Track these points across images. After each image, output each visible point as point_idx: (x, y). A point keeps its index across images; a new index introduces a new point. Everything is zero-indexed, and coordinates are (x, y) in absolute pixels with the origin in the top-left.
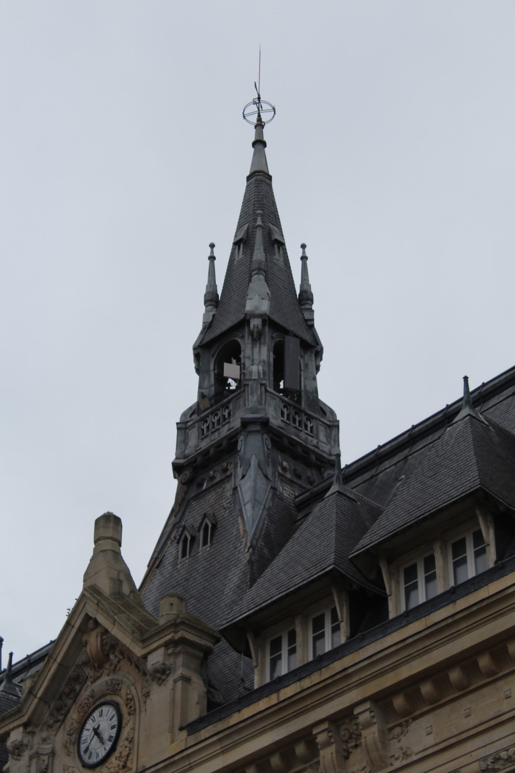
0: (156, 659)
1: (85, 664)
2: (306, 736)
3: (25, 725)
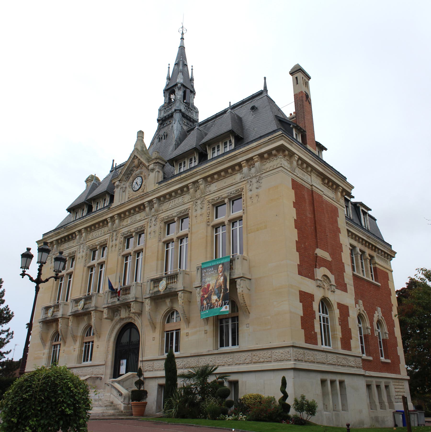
0: (151, 166)
1: (134, 167)
2: (187, 186)
3: (119, 181)
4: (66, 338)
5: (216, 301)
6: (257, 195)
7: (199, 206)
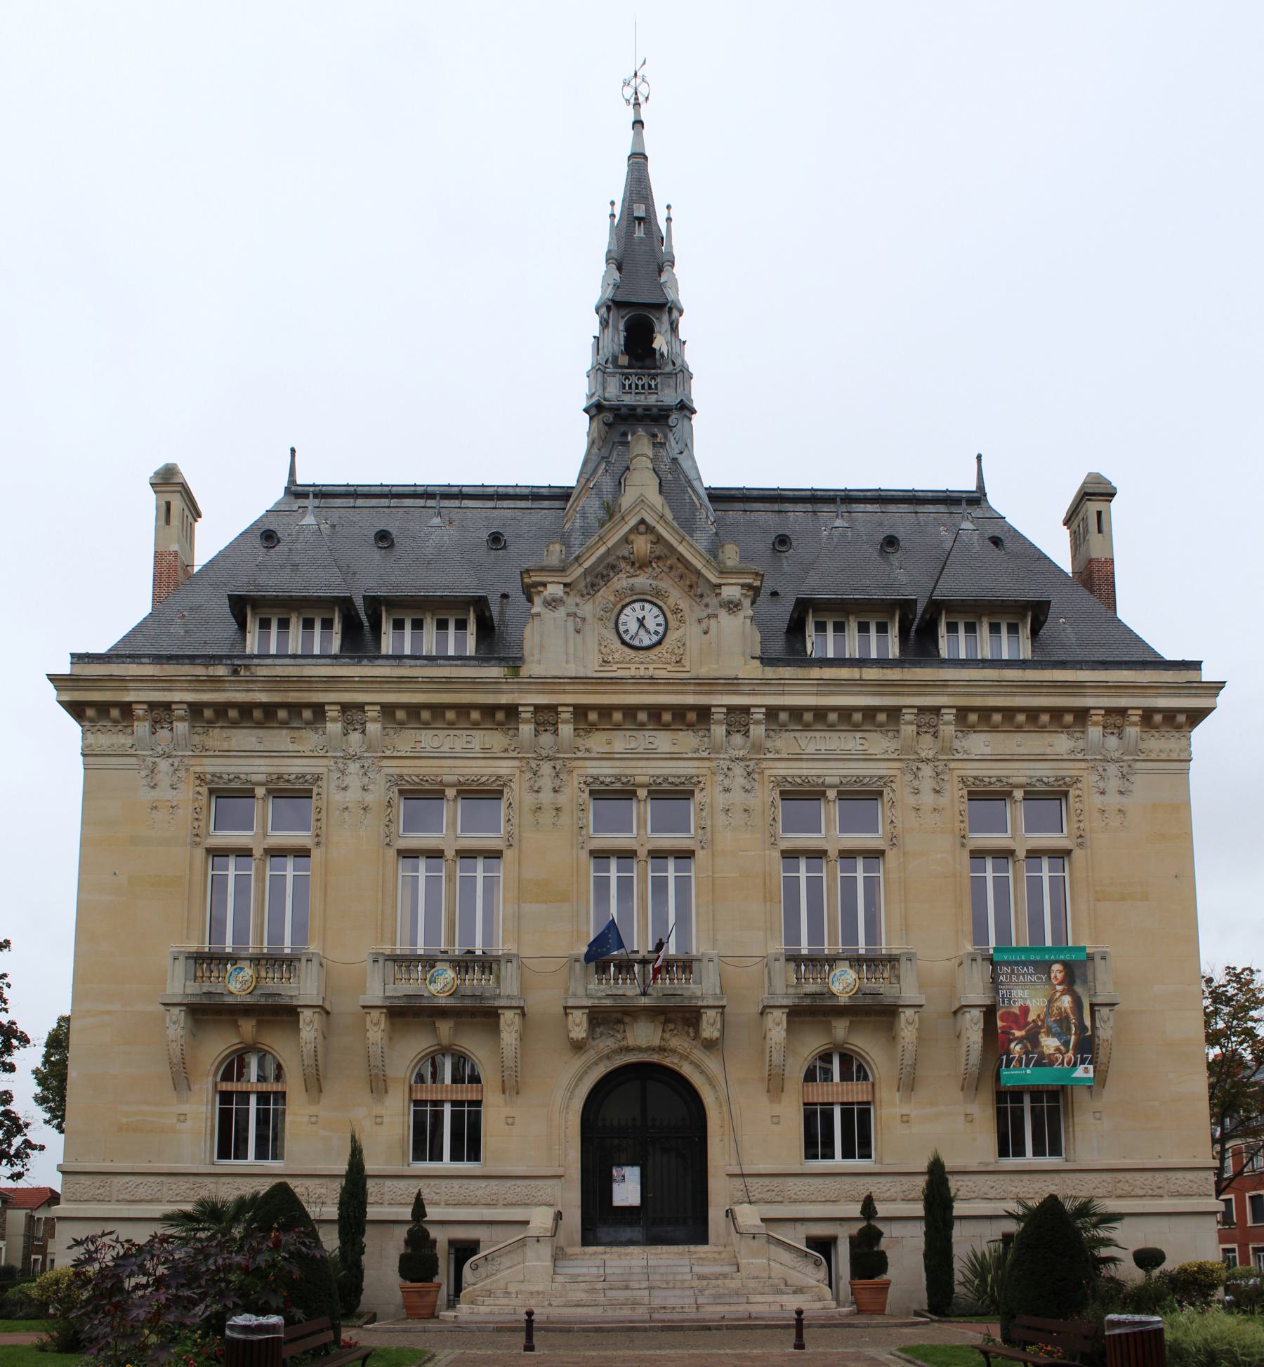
1: (624, 558)
2: (894, 713)
5: (1058, 1050)
7: (927, 784)
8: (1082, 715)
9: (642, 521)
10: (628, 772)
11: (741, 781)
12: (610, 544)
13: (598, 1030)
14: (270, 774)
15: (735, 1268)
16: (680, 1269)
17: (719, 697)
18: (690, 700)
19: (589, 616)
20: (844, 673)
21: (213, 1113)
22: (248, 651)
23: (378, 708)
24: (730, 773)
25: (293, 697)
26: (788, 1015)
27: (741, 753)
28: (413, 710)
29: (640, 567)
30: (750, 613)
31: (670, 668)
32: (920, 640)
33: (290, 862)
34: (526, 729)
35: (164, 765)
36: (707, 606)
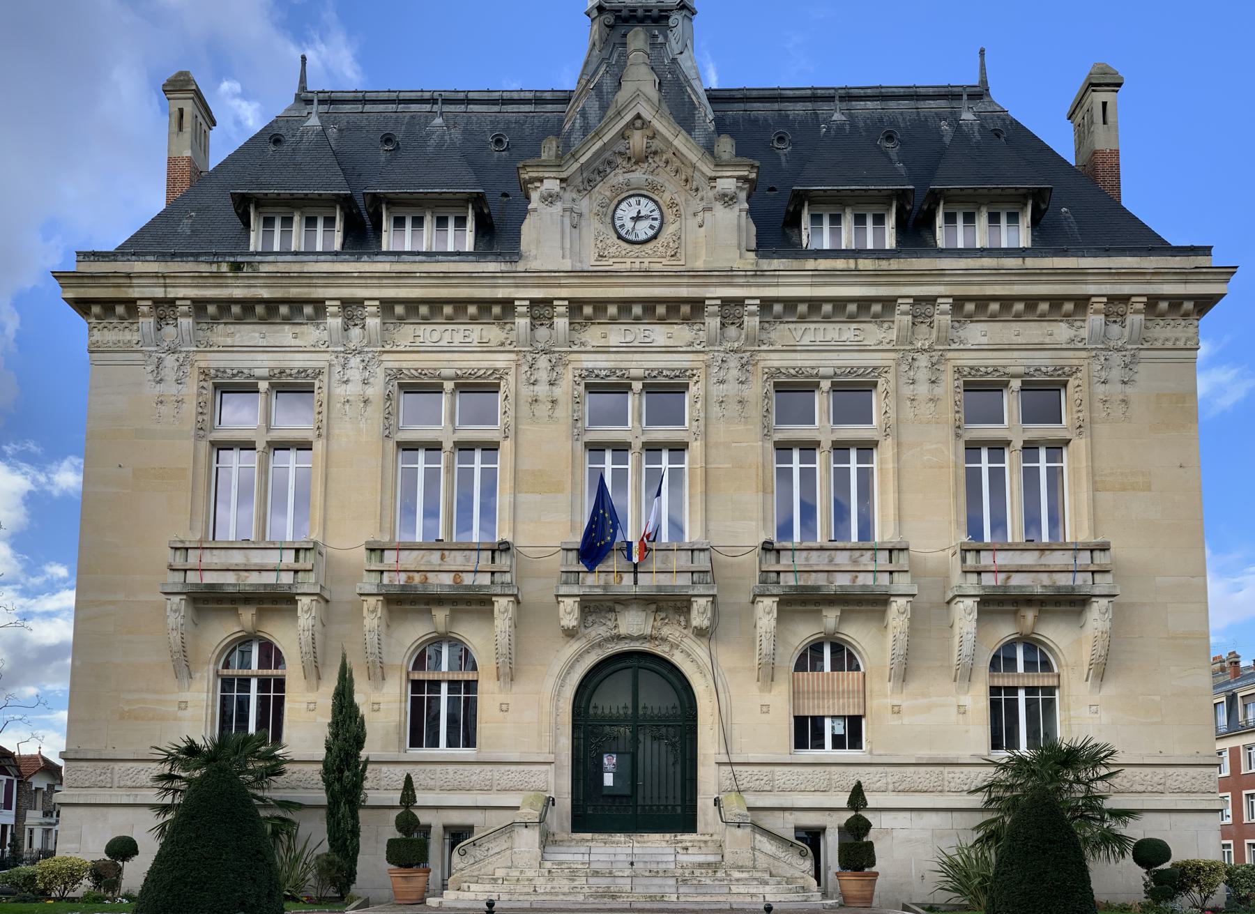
1: (620, 154)
2: (889, 303)
3: (562, 180)
4: (324, 664)
6: (1123, 401)
7: (923, 375)
8: (1082, 302)
9: (638, 116)
10: (623, 365)
11: (735, 373)
12: (606, 139)
13: (590, 619)
14: (272, 369)
15: (719, 858)
16: (665, 858)
17: (712, 289)
18: (684, 292)
19: (585, 211)
20: (840, 264)
21: (214, 700)
22: (252, 249)
23: (377, 303)
24: (725, 365)
25: (294, 292)
26: (779, 603)
27: (736, 345)
28: (412, 305)
29: (636, 163)
30: (746, 206)
31: (665, 261)
32: (915, 232)
33: (292, 455)
34: (523, 323)
35: (170, 360)
36: (702, 199)
